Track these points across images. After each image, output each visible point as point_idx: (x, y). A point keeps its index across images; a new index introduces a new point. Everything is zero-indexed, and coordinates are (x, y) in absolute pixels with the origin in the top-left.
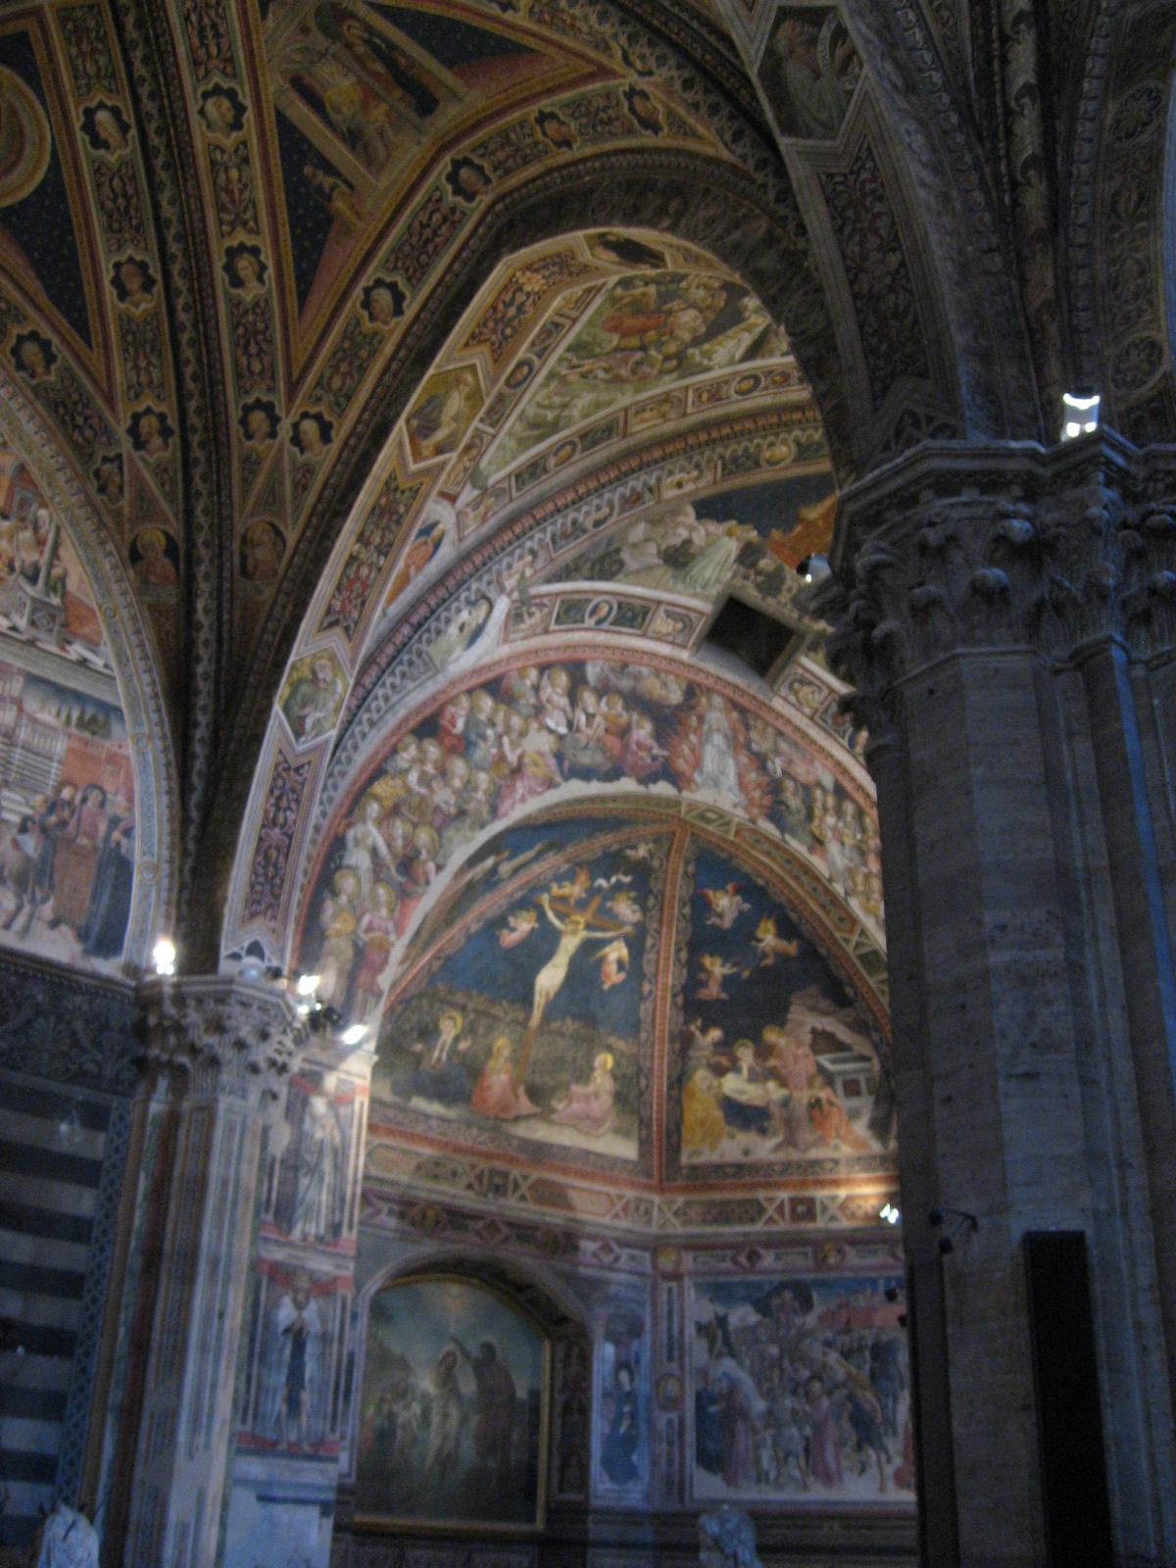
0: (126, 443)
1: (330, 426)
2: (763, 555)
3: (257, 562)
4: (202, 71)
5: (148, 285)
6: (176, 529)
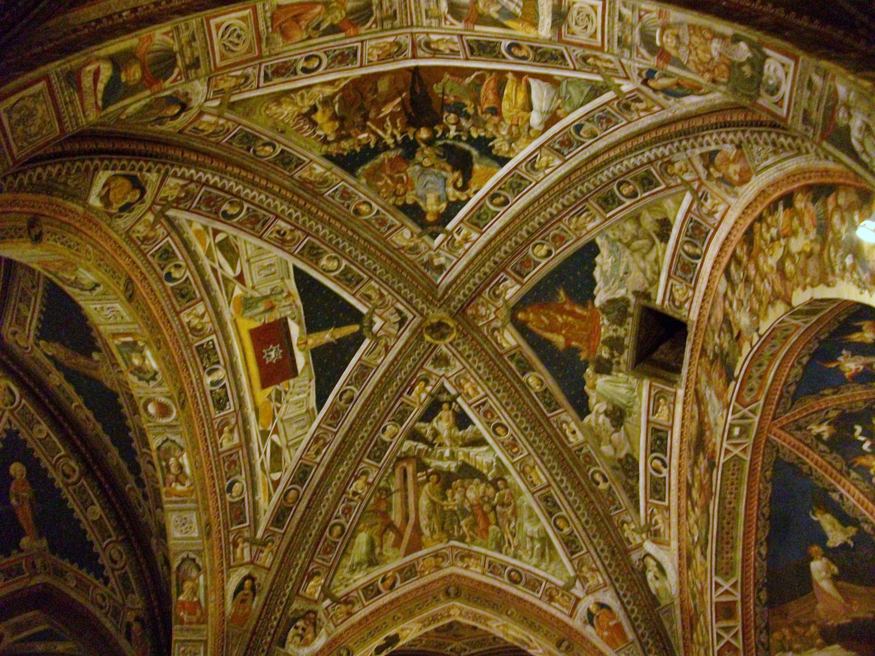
2: (600, 357)
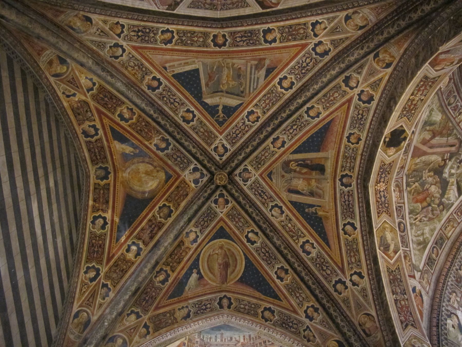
0: (307, 321)
1: (360, 273)
3: (369, 329)
4: (266, 205)
5: (286, 272)
6: (338, 337)
